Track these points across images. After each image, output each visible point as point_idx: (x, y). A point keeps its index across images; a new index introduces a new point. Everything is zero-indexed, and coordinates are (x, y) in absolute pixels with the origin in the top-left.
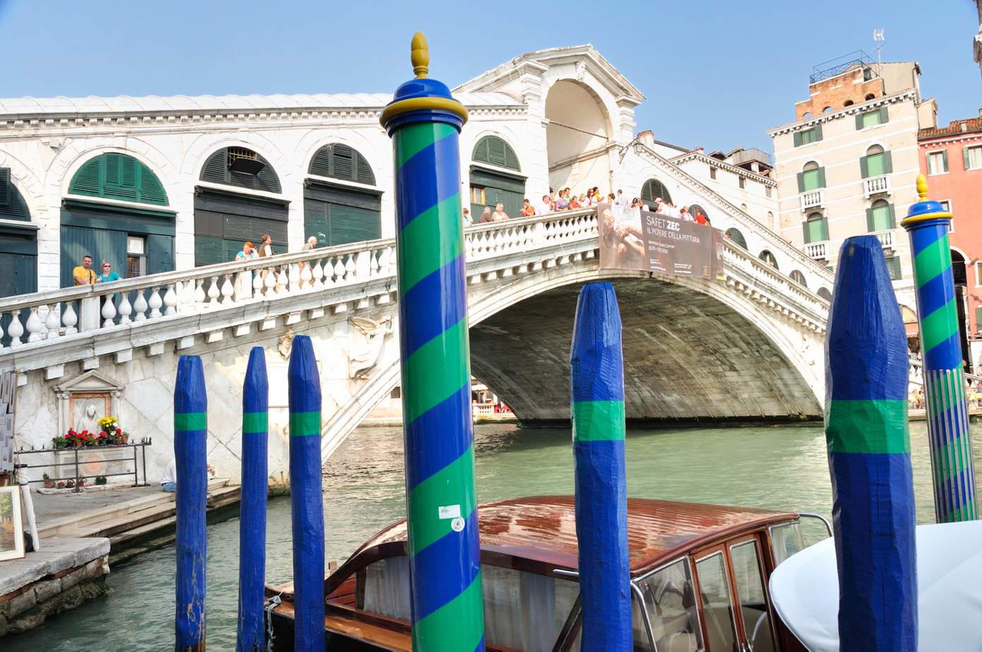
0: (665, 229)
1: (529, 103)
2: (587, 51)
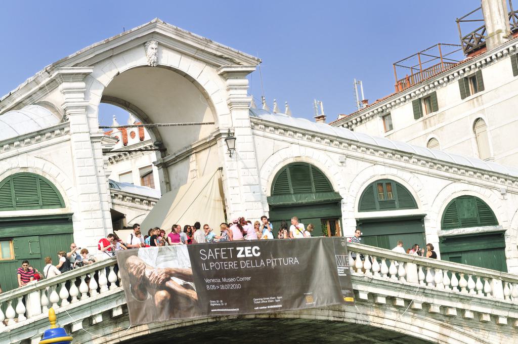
0: (235, 258)
1: (71, 119)
2: (155, 27)
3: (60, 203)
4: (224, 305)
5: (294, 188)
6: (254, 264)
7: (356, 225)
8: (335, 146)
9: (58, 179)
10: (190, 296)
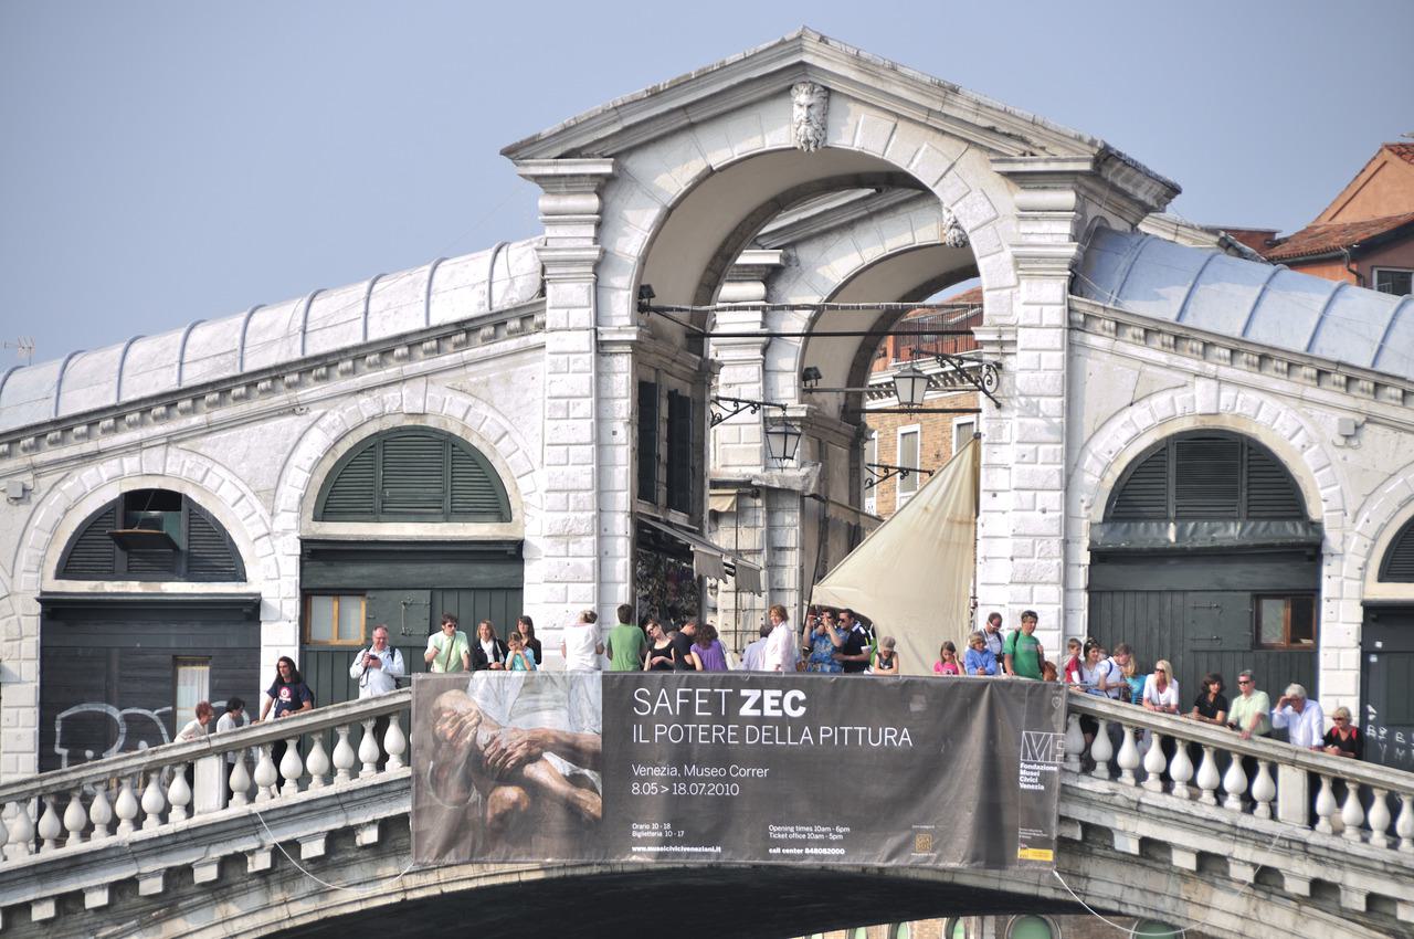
0: (732, 715)
2: (801, 50)
3: (501, 511)
4: (675, 837)
5: (1182, 502)
6: (783, 737)
7: (1361, 620)
8: (1336, 388)
9: (504, 445)
10: (582, 805)
